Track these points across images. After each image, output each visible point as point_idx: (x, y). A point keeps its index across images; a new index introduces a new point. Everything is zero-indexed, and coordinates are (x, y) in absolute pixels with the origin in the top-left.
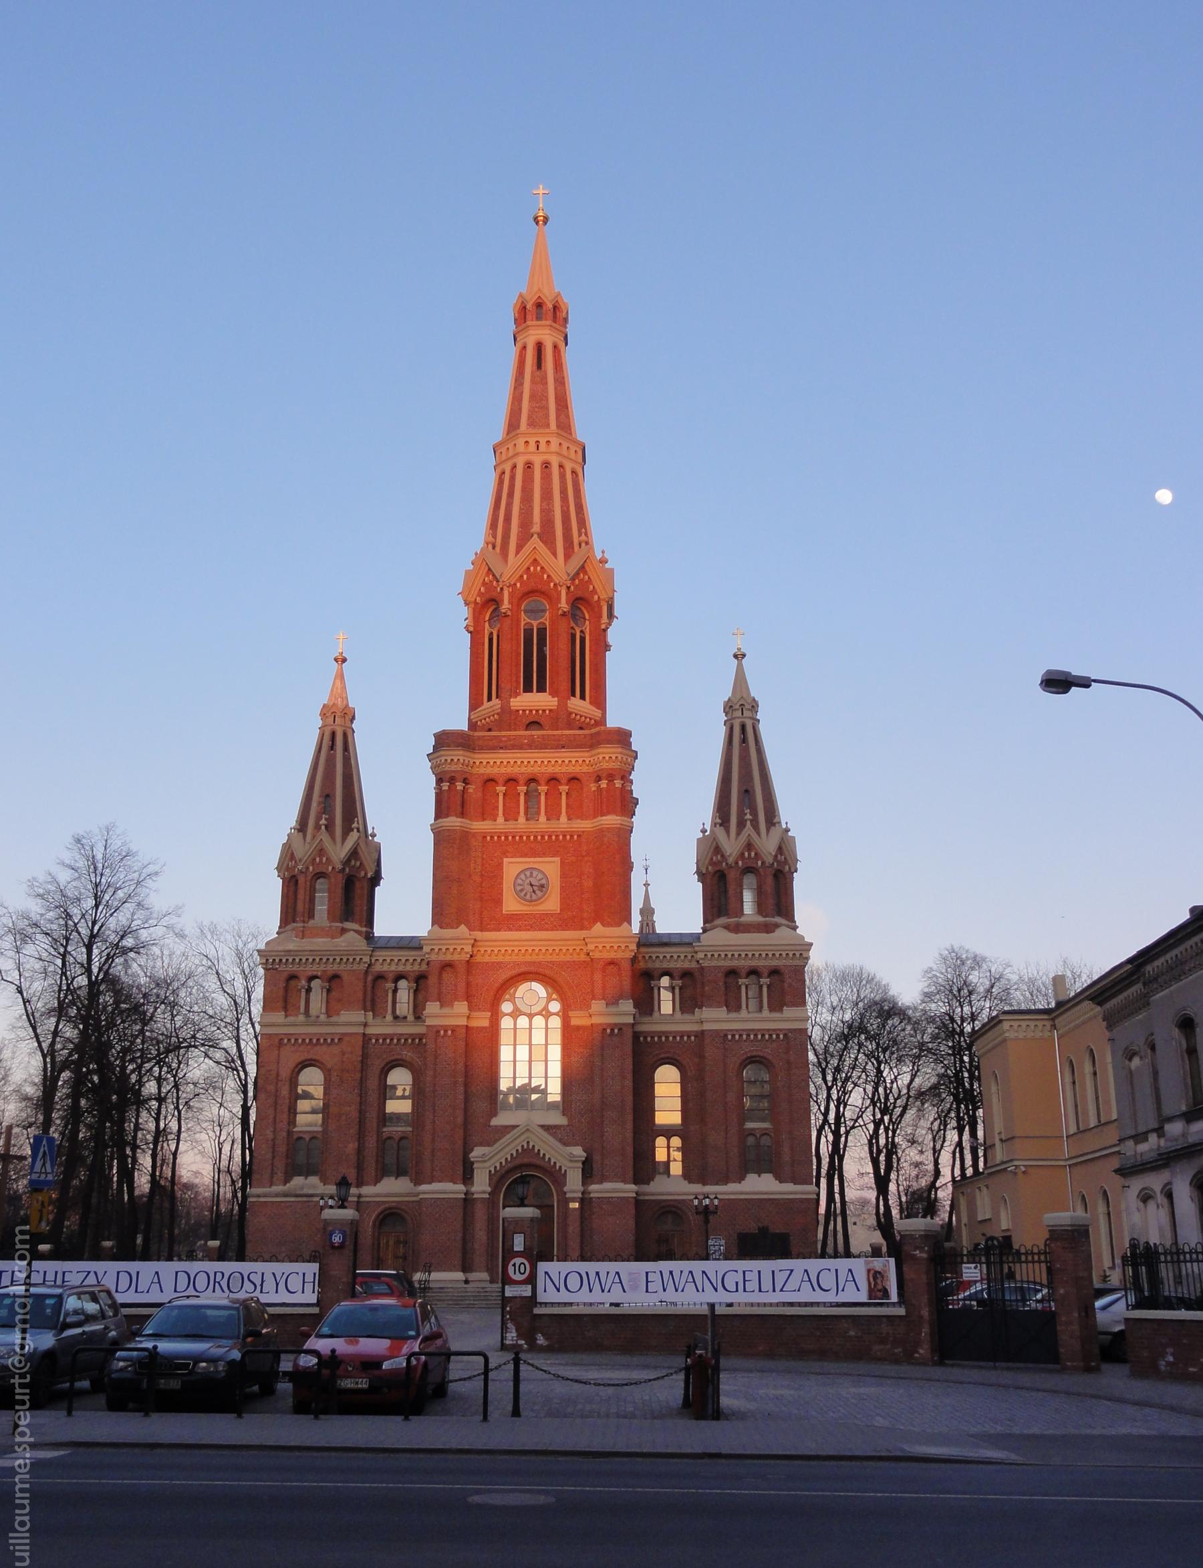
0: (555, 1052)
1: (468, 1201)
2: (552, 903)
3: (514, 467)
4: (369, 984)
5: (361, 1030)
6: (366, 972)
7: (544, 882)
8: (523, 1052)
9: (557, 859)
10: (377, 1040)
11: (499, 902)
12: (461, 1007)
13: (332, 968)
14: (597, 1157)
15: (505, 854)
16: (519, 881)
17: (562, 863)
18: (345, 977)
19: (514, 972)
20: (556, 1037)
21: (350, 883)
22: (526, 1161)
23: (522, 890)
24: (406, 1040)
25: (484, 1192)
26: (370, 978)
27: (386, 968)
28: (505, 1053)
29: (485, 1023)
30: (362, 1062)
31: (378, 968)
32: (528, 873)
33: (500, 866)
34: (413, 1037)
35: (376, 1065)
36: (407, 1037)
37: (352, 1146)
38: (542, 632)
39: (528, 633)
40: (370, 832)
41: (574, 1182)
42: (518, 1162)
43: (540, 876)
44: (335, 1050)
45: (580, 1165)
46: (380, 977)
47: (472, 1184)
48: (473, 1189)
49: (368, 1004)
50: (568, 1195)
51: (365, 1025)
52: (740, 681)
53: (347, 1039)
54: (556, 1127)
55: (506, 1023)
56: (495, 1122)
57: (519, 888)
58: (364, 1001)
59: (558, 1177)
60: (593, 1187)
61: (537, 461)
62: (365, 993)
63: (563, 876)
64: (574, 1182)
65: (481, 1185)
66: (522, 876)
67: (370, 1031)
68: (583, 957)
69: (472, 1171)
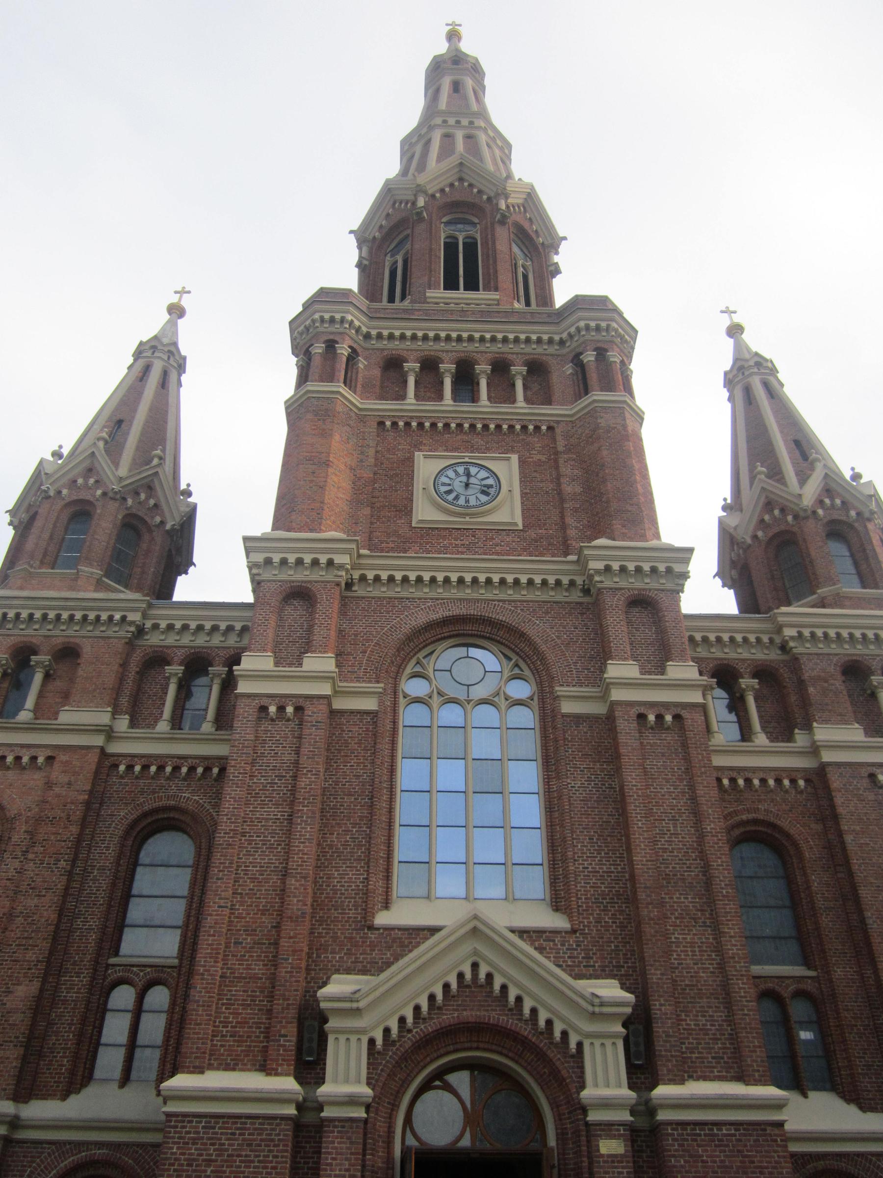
0: (526, 776)
1: (307, 1129)
2: (509, 511)
3: (428, 142)
4: (133, 668)
5: (98, 741)
6: (131, 644)
7: (490, 481)
8: (451, 774)
9: (515, 458)
10: (130, 767)
11: (406, 509)
12: (320, 663)
13: (61, 635)
14: (661, 1007)
15: (418, 446)
16: (444, 479)
17: (522, 463)
18: (87, 650)
19: (434, 616)
20: (529, 744)
21: (133, 527)
22: (469, 1015)
23: (449, 492)
24: (192, 769)
25: (352, 1101)
26: (137, 657)
27: (171, 640)
28: (409, 773)
29: (370, 704)
30: (88, 804)
31: (154, 639)
32: (461, 470)
33: (409, 462)
34: (208, 762)
35: (119, 816)
36: (193, 762)
37: (25, 991)
38: (471, 247)
39: (451, 247)
40: (183, 486)
41: (605, 1084)
42: (448, 1017)
43: (483, 474)
44: (36, 779)
45: (619, 1029)
46: (157, 660)
47: (321, 1080)
48: (326, 1090)
49: (124, 701)
50: (593, 1116)
51: (110, 733)
52: (740, 348)
53: (62, 757)
54: (540, 932)
55: (410, 715)
56: (382, 919)
57: (443, 489)
58: (118, 691)
59: (561, 1068)
60: (662, 1091)
61: (459, 135)
62: (121, 679)
63: (524, 479)
64: (605, 1084)
65: (346, 1081)
66: (451, 473)
67: (115, 748)
68: (576, 596)
69: (323, 1039)
